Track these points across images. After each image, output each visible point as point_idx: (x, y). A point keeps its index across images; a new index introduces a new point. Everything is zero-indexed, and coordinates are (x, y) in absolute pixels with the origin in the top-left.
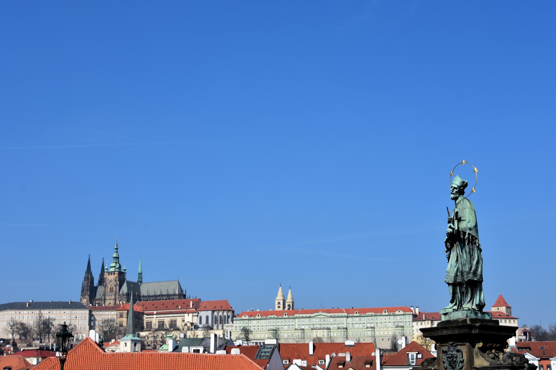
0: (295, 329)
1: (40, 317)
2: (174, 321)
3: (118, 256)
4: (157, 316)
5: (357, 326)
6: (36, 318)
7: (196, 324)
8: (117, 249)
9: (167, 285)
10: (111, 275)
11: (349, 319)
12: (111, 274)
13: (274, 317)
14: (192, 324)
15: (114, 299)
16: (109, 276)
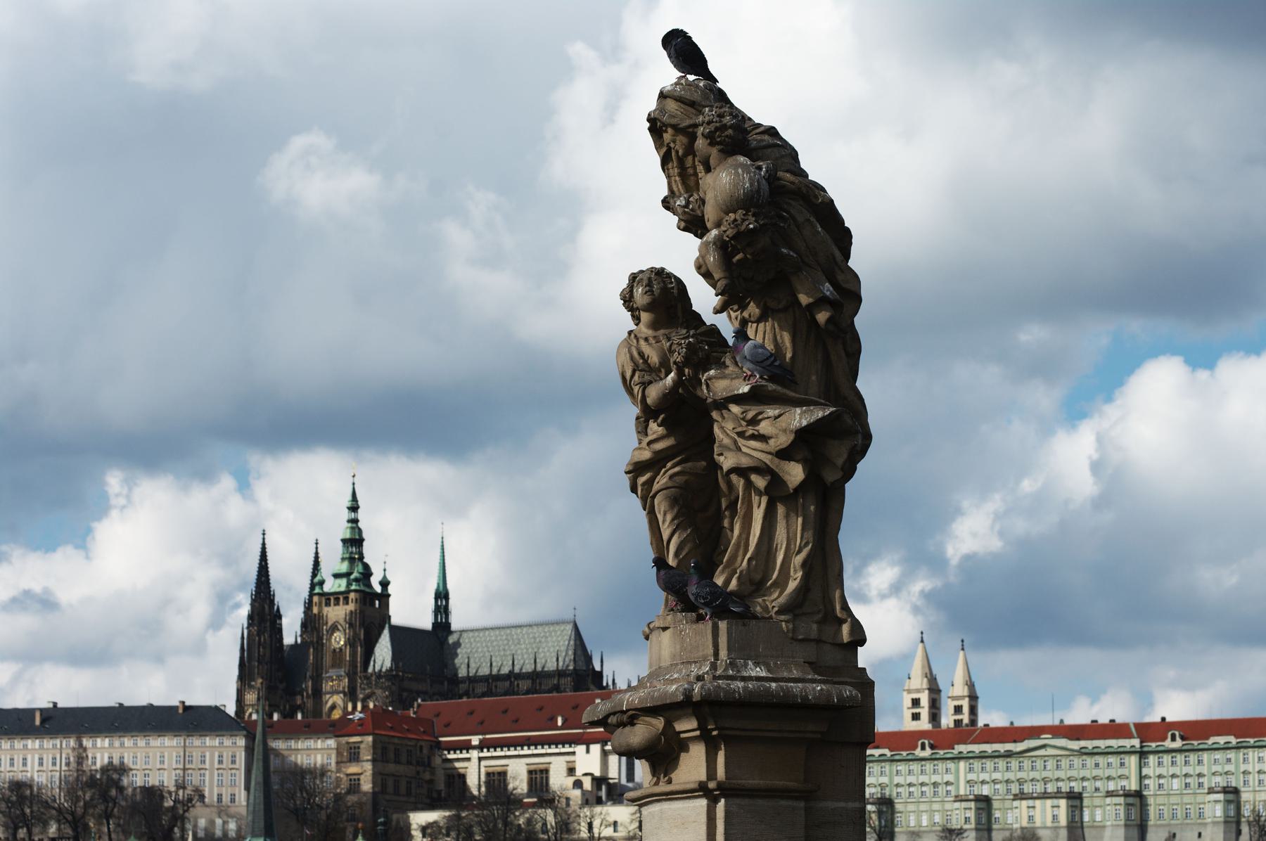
0: (956, 797)
1: (81, 760)
2: (541, 771)
3: (357, 537)
4: (482, 755)
5: (1176, 784)
6: (68, 764)
7: (616, 781)
8: (354, 508)
9: (535, 638)
10: (335, 605)
11: (1152, 759)
12: (337, 600)
13: (885, 755)
14: (599, 781)
15: (346, 690)
16: (326, 610)
